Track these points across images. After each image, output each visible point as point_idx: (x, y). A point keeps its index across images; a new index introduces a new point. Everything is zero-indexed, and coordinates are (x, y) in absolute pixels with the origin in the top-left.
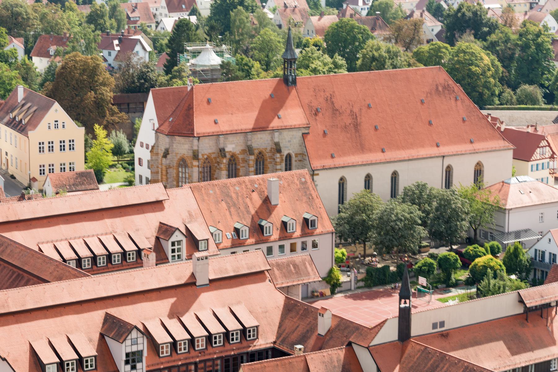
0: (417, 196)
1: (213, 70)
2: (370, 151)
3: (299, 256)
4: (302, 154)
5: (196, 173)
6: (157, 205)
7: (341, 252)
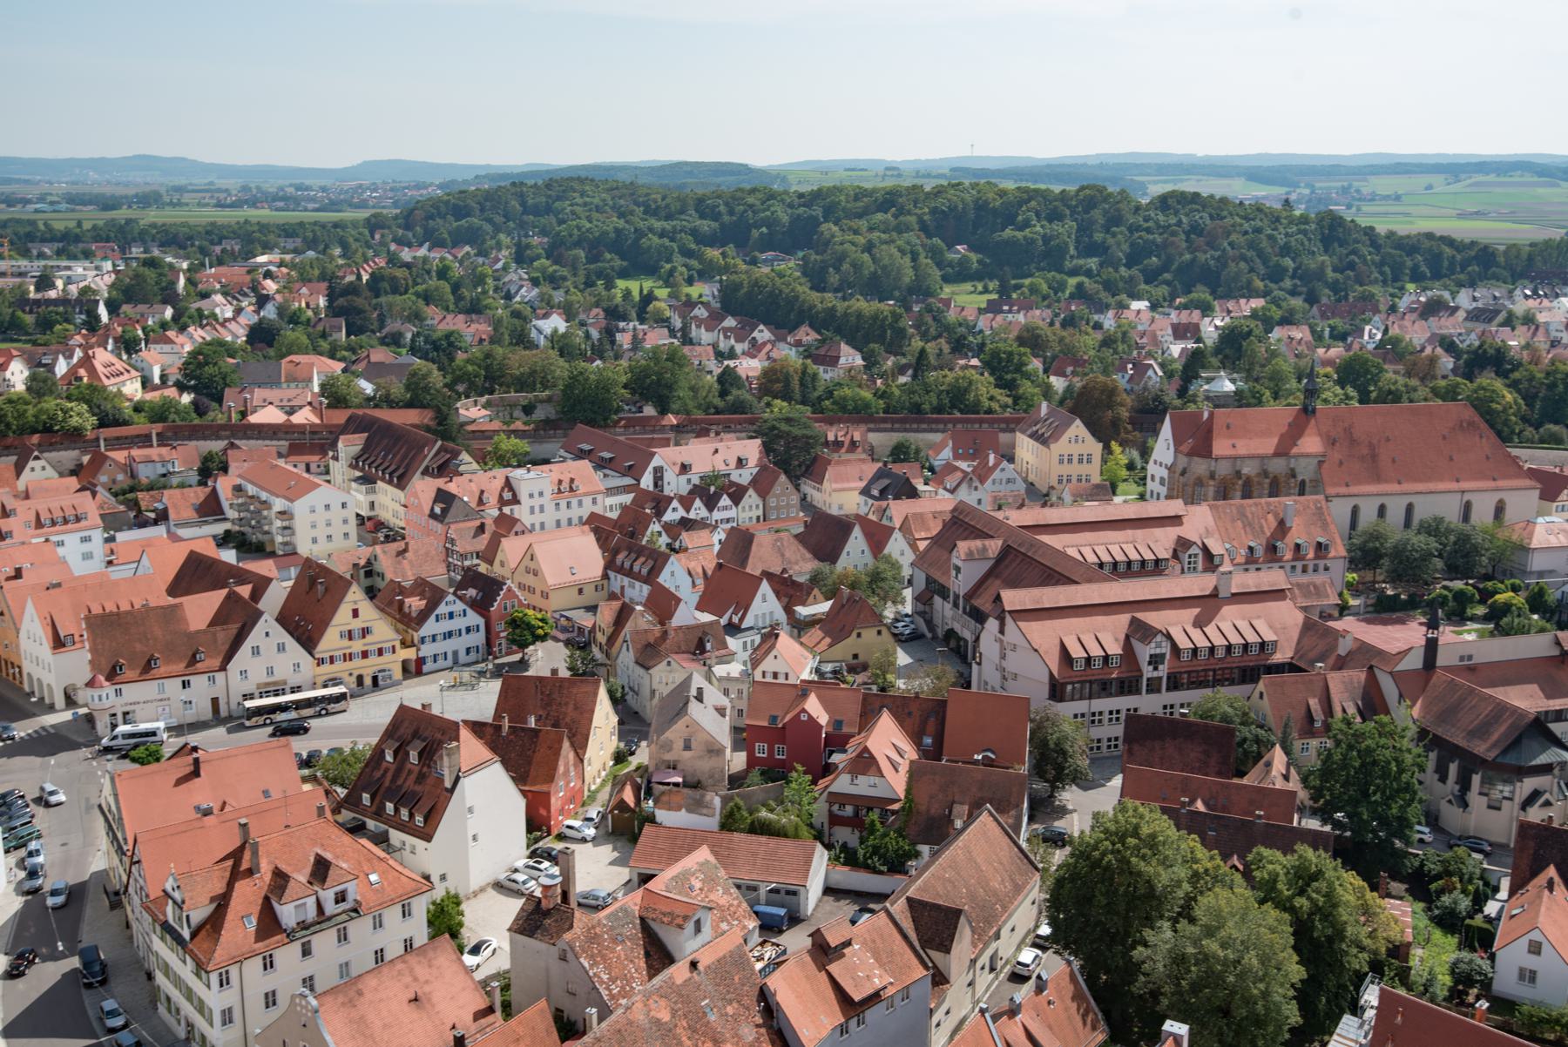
0: (1433, 528)
1: (1226, 395)
2: (1387, 481)
3: (1320, 578)
4: (1316, 481)
5: (1211, 491)
6: (1176, 520)
7: (1352, 576)
